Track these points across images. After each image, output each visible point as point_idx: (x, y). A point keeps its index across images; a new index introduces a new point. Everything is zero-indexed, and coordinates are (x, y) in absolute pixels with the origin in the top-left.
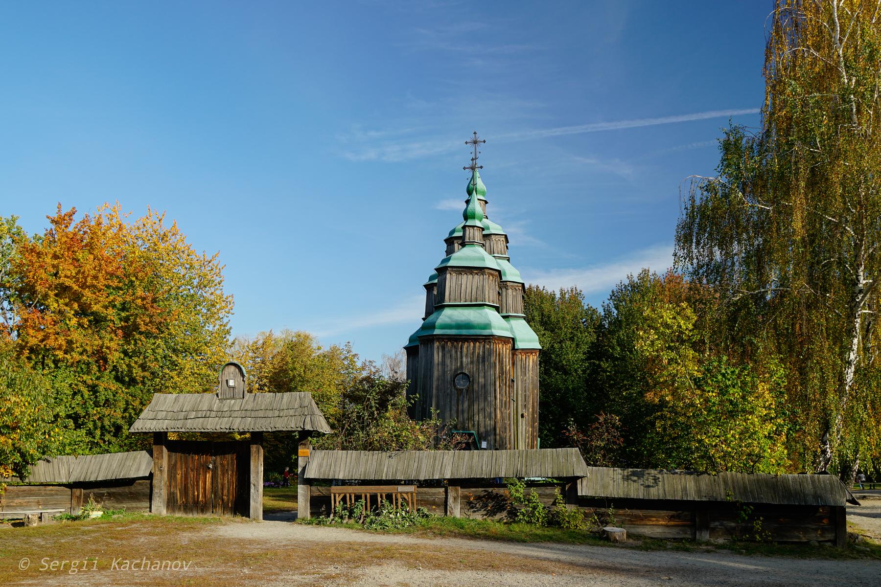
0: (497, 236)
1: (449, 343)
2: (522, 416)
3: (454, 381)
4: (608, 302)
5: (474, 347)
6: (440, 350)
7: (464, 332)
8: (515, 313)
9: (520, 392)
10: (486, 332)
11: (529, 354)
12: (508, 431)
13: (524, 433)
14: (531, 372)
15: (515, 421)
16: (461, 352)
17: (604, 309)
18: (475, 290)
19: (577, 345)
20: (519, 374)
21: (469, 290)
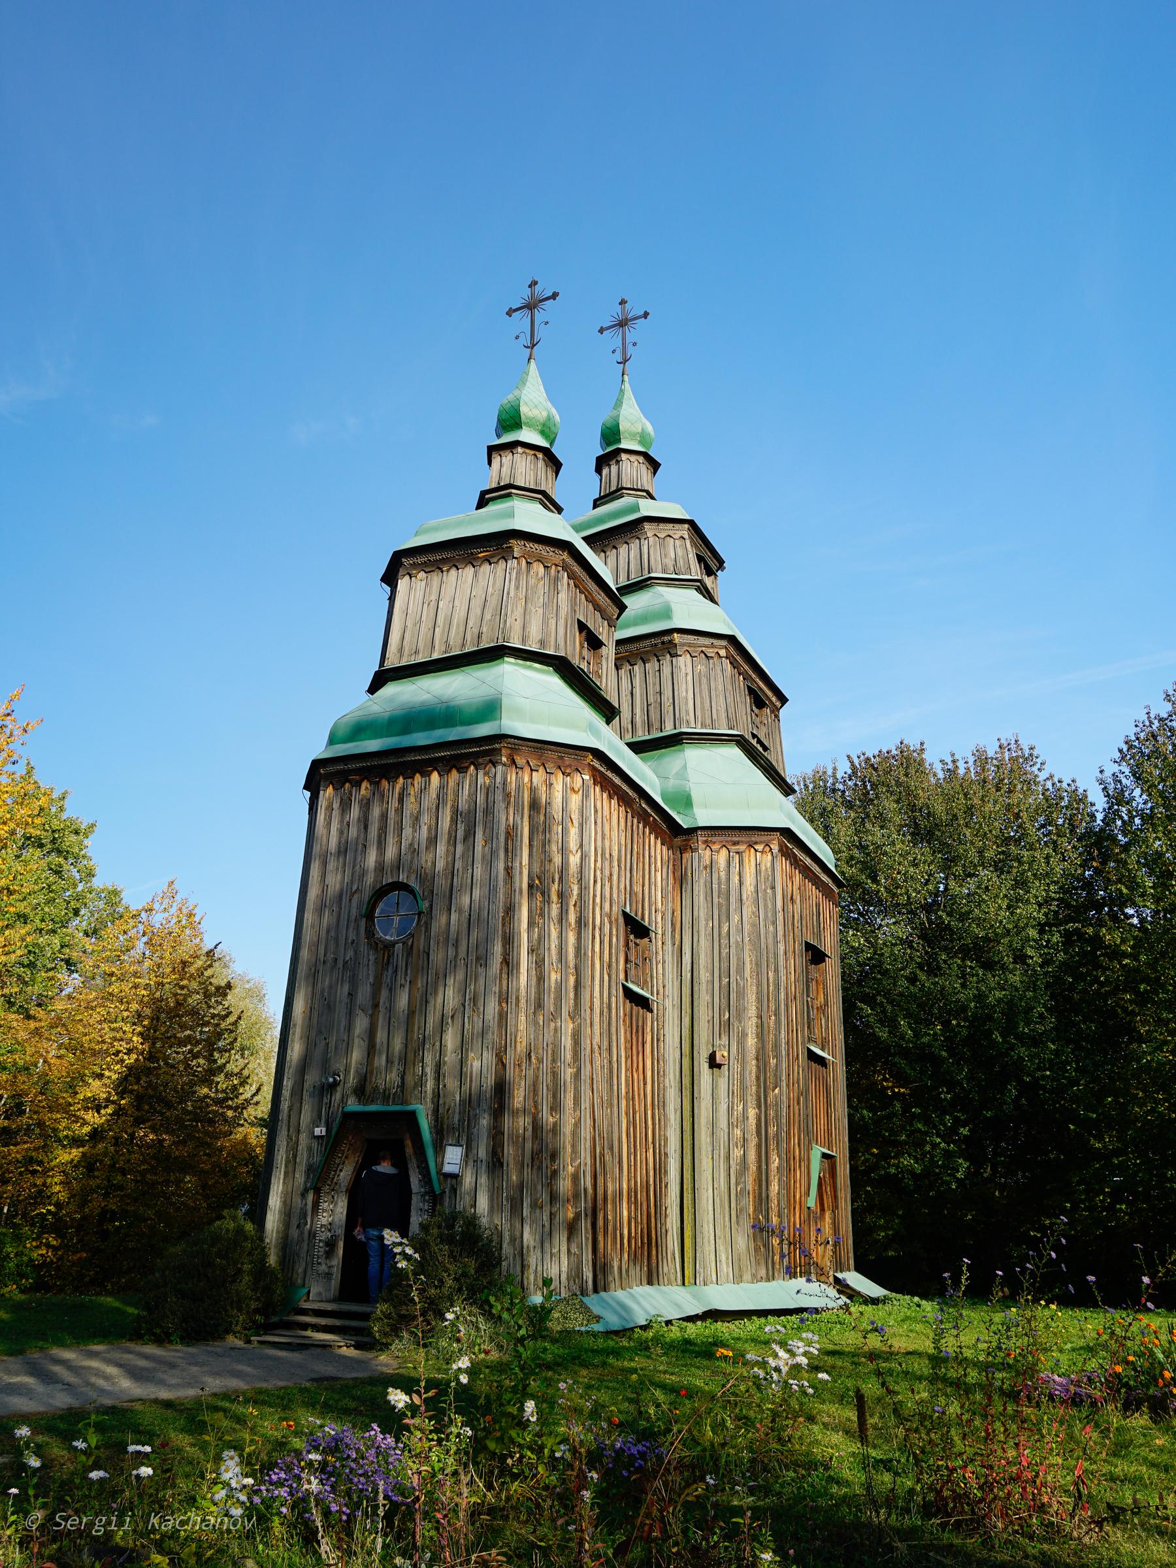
0: (662, 526)
1: (365, 784)
2: (713, 1064)
3: (370, 916)
4: (1115, 768)
5: (442, 787)
6: (336, 813)
7: (421, 739)
8: (703, 725)
9: (703, 975)
10: (483, 730)
11: (742, 848)
12: (568, 1101)
13: (723, 1123)
14: (748, 910)
15: (686, 1081)
16: (400, 811)
17: (1105, 789)
18: (479, 612)
19: (1021, 883)
20: (702, 912)
21: (459, 614)
